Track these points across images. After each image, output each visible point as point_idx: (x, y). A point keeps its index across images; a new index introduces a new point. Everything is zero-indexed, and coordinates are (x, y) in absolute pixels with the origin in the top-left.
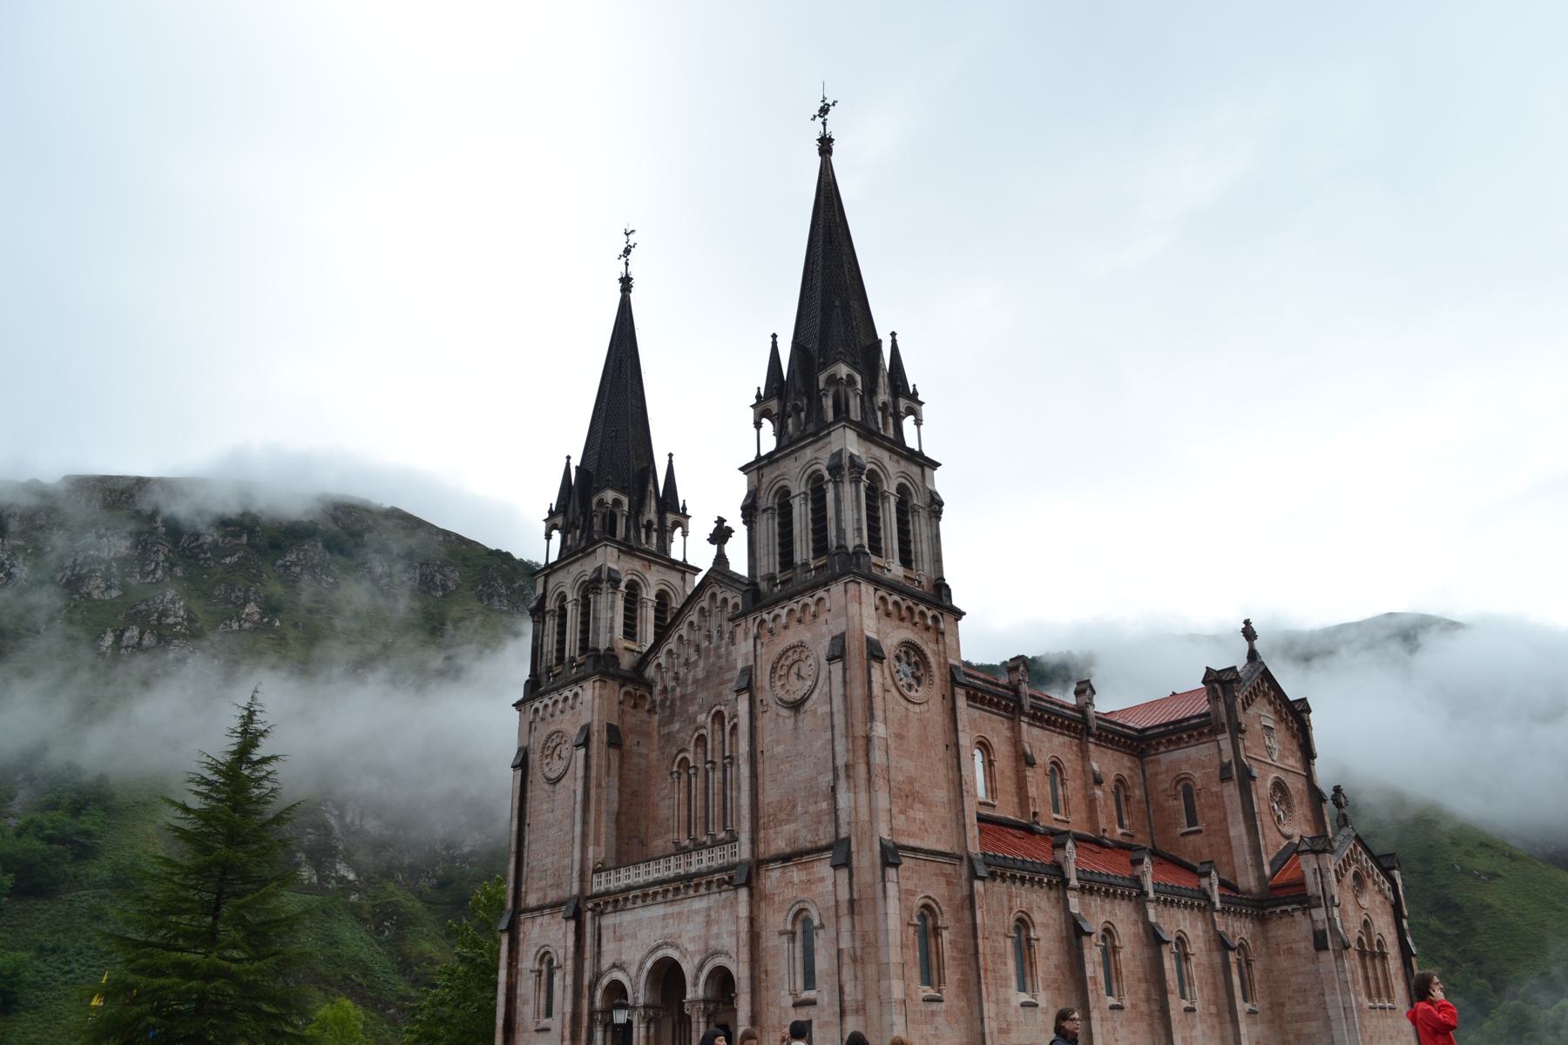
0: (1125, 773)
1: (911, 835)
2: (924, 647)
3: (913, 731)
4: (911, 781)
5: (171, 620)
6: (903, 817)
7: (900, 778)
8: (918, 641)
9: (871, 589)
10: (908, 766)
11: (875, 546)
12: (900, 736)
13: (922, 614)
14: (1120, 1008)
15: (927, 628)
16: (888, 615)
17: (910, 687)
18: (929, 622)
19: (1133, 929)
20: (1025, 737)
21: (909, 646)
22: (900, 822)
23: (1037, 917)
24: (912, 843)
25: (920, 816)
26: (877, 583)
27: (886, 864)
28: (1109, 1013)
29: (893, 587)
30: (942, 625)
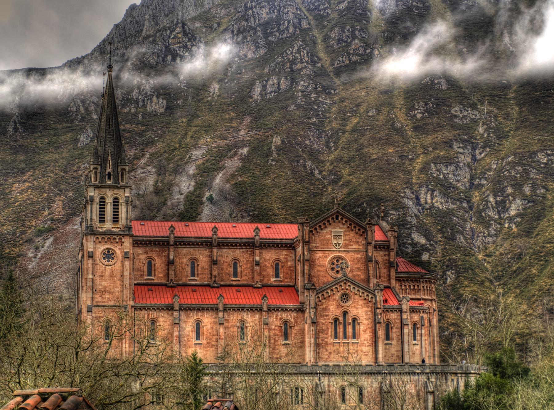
0: (282, 257)
1: (104, 302)
2: (115, 249)
3: (107, 273)
4: (105, 287)
5: (299, 66)
6: (100, 298)
7: (100, 287)
8: (111, 247)
9: (92, 237)
10: (105, 284)
11: (102, 220)
12: (102, 276)
13: (115, 238)
14: (201, 344)
15: (117, 242)
16: (100, 242)
17: (108, 261)
18: (117, 240)
19: (213, 320)
20: (215, 254)
21: (109, 250)
22: (100, 299)
23: (161, 319)
24: (103, 304)
25: (108, 296)
26: (95, 235)
27: (90, 310)
28: (194, 346)
29: (101, 234)
30: (123, 240)
